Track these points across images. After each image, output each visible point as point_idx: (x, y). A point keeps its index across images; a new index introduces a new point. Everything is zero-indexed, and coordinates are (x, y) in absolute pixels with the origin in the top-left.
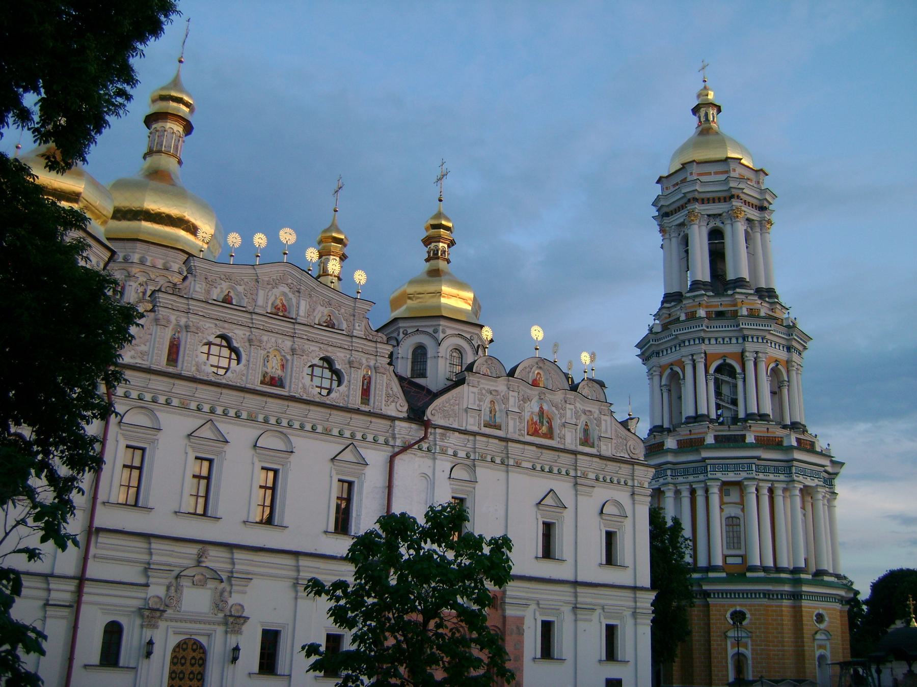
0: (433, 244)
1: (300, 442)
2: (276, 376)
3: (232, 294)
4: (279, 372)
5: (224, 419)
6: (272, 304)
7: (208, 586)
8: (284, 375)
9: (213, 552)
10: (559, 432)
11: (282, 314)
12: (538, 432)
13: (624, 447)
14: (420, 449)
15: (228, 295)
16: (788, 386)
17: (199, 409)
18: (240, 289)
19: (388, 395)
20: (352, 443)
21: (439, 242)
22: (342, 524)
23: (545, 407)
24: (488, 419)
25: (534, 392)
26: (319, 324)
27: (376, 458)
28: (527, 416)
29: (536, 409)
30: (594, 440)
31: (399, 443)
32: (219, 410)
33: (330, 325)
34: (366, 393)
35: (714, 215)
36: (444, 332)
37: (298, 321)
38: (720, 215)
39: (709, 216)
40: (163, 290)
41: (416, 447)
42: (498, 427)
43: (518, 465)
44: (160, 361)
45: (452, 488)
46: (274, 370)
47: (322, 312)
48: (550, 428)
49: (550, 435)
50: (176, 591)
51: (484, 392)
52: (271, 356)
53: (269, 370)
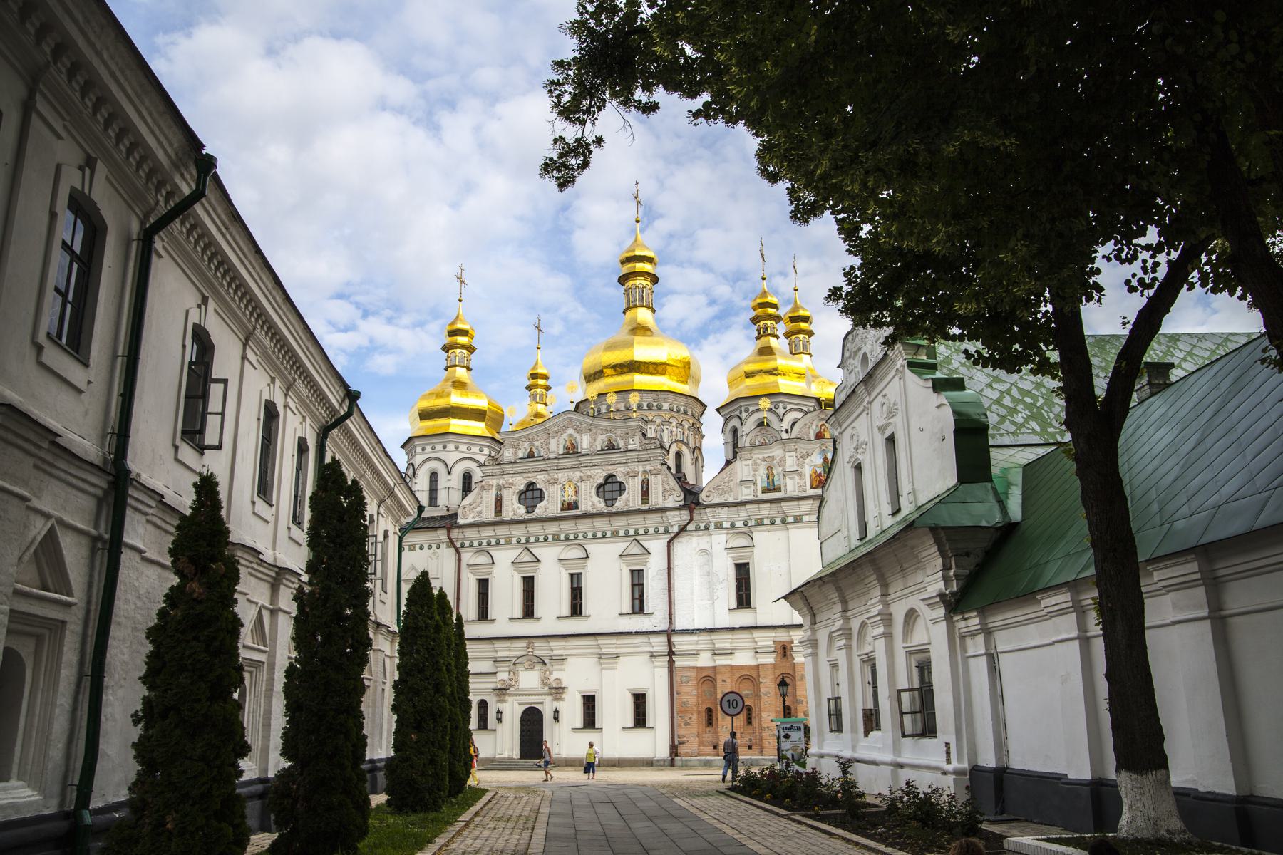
0: (762, 323)
1: (594, 548)
3: (534, 450)
4: (574, 498)
5: (537, 545)
9: (537, 643)
11: (571, 452)
14: (697, 529)
17: (519, 542)
18: (537, 444)
19: (665, 491)
22: (639, 606)
25: (816, 445)
26: (602, 450)
27: (657, 546)
28: (808, 471)
29: (819, 461)
31: (676, 529)
32: (532, 539)
33: (611, 447)
34: (645, 494)
40: (486, 464)
42: (779, 490)
43: (798, 520)
44: (489, 515)
45: (732, 557)
50: (514, 674)
51: (758, 461)
52: (567, 487)
53: (566, 499)
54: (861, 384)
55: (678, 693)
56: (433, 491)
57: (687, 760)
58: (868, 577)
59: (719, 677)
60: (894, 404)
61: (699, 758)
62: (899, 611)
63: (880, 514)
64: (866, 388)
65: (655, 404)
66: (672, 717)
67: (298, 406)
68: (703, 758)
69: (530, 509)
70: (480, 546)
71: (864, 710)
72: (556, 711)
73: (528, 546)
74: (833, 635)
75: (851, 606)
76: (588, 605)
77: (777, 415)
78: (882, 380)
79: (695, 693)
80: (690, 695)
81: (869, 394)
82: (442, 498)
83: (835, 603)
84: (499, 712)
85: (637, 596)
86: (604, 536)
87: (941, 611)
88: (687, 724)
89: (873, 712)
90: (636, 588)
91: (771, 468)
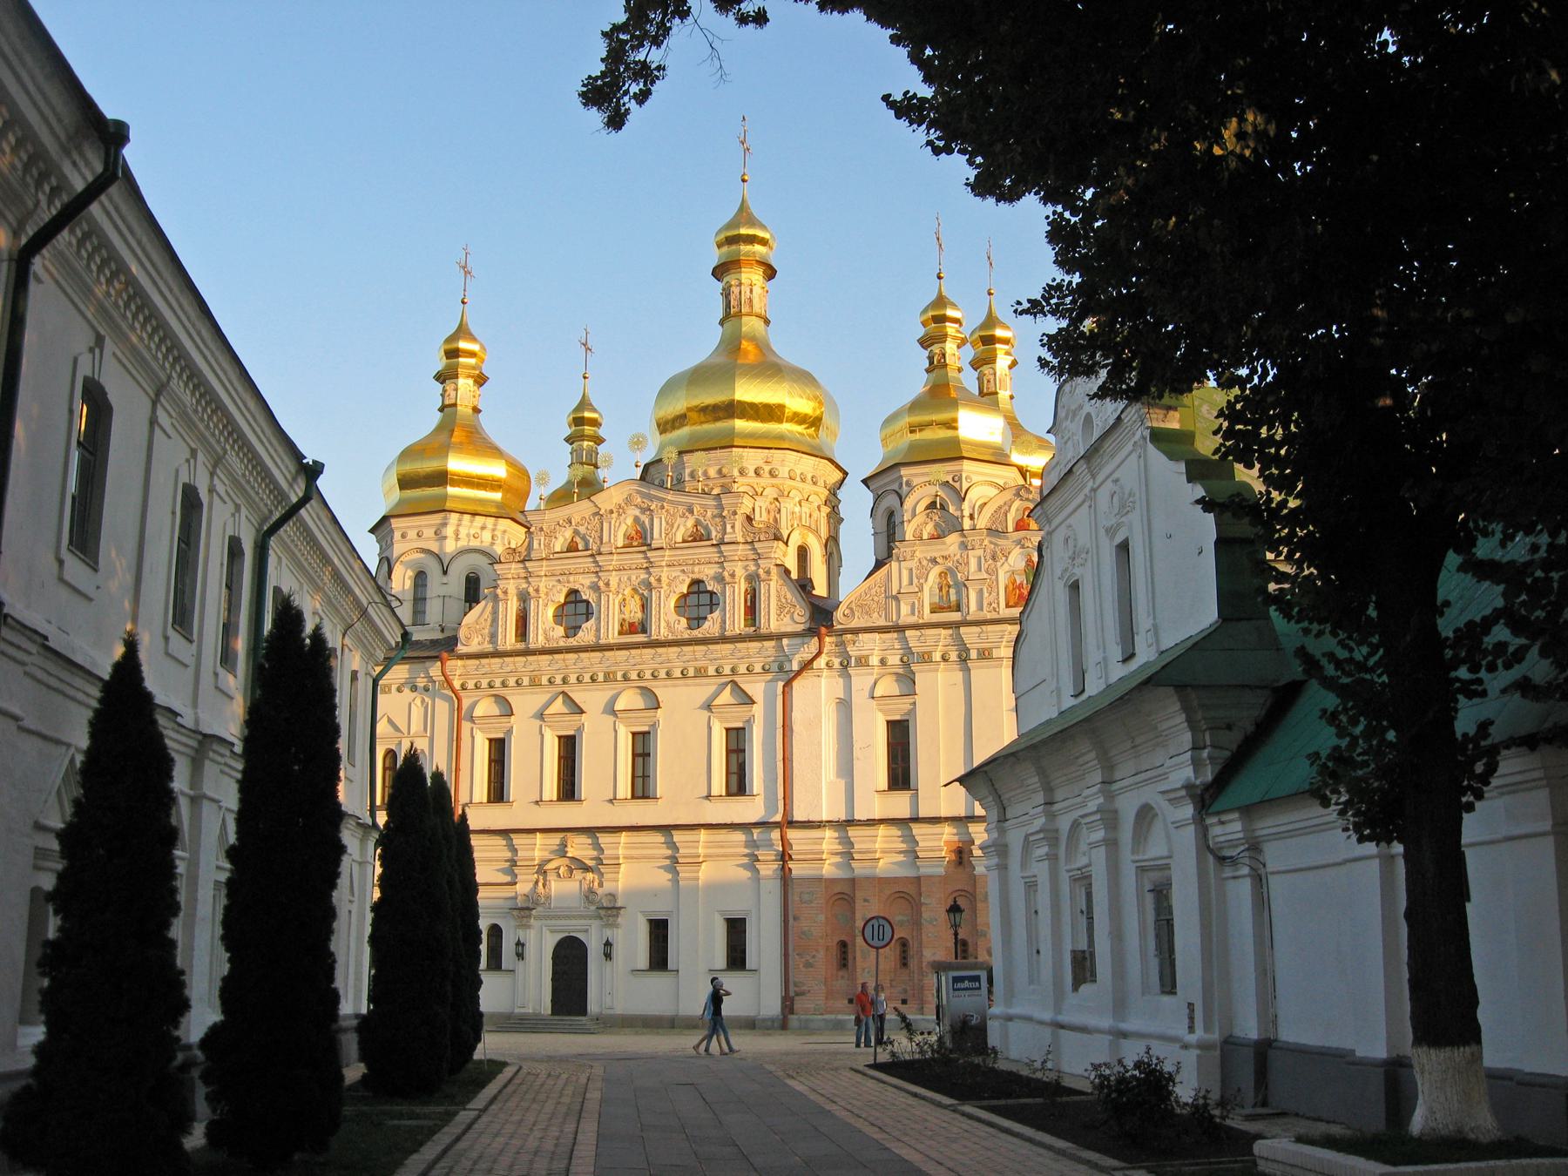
3: (578, 539)
11: (635, 543)
19: (781, 608)
20: (733, 682)
21: (932, 344)
22: (738, 784)
26: (684, 541)
31: (795, 667)
32: (573, 679)
34: (752, 610)
44: (509, 640)
46: (632, 614)
47: (684, 527)
50: (544, 886)
53: (627, 617)
54: (1082, 462)
55: (795, 919)
56: (419, 600)
57: (807, 1020)
58: (1084, 754)
59: (859, 895)
60: (1130, 495)
61: (826, 1017)
62: (1128, 807)
63: (1105, 659)
64: (1089, 468)
65: (767, 468)
66: (786, 955)
67: (229, 490)
68: (833, 1017)
70: (491, 687)
71: (1073, 952)
72: (608, 944)
73: (566, 689)
74: (1031, 838)
75: (1059, 795)
77: (957, 492)
78: (1112, 456)
79: (822, 918)
80: (816, 922)
81: (1094, 477)
82: (433, 611)
83: (1034, 791)
84: (519, 944)
85: (734, 768)
87: (1188, 811)
88: (808, 965)
89: (1087, 955)
90: (734, 757)
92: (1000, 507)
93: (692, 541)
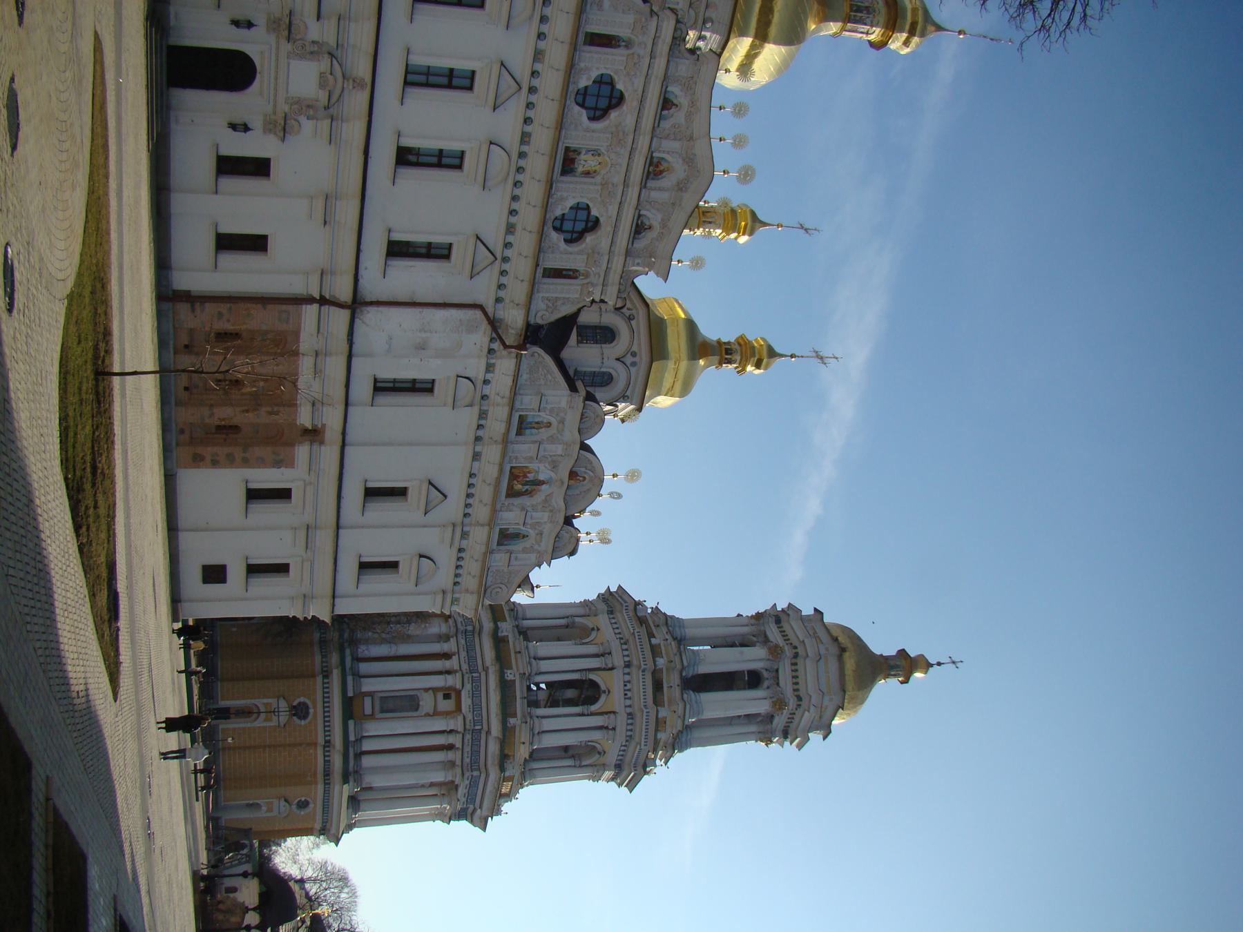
2: (576, 166)
3: (673, 110)
4: (580, 169)
6: (663, 159)
7: (320, 91)
8: (577, 174)
9: (362, 97)
10: (516, 504)
11: (650, 170)
12: (514, 480)
13: (499, 581)
14: (492, 340)
15: (674, 105)
16: (575, 766)
22: (398, 250)
23: (544, 487)
24: (528, 420)
26: (639, 216)
27: (483, 289)
28: (533, 466)
29: (541, 477)
30: (506, 545)
34: (558, 273)
35: (778, 678)
36: (634, 364)
37: (644, 190)
38: (778, 684)
39: (777, 671)
41: (494, 335)
42: (520, 432)
43: (476, 456)
46: (583, 162)
47: (653, 217)
48: (519, 494)
49: (512, 493)
52: (600, 159)
53: (582, 157)
68: (172, 336)
69: (582, 98)
76: (410, 175)
80: (261, 319)
86: (513, 212)
88: (220, 315)
91: (549, 427)
92: (591, 463)
93: (637, 224)
